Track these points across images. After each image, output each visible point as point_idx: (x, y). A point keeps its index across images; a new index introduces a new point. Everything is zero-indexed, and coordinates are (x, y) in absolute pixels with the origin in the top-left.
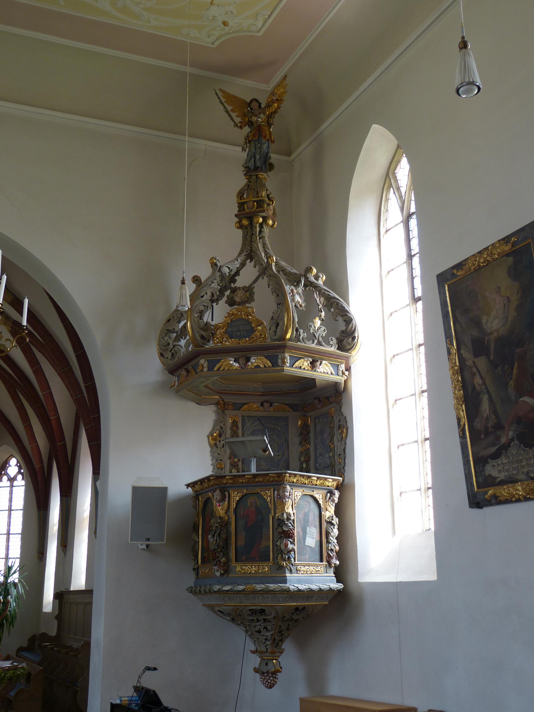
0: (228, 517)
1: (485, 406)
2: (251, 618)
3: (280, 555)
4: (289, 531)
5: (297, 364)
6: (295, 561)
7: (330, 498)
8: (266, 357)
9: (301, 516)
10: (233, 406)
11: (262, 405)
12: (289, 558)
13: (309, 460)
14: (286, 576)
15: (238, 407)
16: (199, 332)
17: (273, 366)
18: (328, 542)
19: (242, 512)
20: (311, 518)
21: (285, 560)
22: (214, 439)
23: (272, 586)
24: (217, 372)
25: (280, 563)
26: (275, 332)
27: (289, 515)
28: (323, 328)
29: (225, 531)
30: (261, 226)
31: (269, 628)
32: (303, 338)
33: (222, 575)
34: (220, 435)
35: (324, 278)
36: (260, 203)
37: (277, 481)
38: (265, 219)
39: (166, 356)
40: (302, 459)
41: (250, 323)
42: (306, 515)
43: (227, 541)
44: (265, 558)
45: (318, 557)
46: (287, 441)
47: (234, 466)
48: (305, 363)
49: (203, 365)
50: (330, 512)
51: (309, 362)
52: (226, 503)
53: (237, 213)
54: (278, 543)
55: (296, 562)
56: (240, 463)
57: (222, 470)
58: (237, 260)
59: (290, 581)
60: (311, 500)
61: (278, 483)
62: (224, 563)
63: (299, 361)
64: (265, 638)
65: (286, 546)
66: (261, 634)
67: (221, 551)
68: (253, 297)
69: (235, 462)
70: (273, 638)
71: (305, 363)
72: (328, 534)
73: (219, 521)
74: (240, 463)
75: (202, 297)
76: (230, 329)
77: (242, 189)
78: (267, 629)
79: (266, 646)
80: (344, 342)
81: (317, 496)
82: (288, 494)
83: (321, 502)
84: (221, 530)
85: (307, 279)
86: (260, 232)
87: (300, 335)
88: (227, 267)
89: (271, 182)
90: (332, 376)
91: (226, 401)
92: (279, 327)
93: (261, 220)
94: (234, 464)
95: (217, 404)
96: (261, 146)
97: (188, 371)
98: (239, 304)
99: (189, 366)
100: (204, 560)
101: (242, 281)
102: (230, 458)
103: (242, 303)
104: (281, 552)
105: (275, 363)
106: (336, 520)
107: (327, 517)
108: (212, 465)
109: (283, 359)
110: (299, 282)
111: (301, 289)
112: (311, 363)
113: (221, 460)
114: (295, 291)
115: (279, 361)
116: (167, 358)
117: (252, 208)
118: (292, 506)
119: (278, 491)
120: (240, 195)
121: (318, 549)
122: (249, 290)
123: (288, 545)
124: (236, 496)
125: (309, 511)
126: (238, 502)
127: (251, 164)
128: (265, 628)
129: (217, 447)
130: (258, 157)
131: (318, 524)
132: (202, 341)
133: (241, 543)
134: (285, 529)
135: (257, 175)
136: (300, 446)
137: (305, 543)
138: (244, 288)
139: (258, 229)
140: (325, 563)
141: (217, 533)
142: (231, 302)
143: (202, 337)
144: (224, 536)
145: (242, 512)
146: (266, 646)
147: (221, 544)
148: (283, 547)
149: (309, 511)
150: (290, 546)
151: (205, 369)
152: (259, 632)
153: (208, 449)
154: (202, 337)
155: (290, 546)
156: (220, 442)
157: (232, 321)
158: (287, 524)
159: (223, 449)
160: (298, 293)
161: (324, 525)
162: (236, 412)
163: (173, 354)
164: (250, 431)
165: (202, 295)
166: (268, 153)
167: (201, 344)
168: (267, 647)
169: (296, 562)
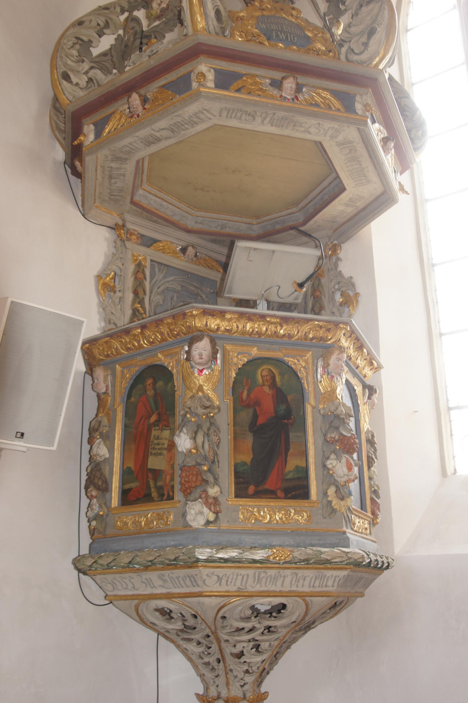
2: (241, 625)
10: (138, 238)
11: (184, 250)
15: (149, 242)
22: (105, 286)
26: (366, 45)
31: (264, 646)
33: (208, 523)
37: (321, 339)
39: (74, 79)
64: (246, 667)
66: (242, 660)
67: (209, 470)
70: (261, 669)
78: (257, 650)
79: (242, 686)
91: (129, 226)
95: (114, 228)
97: (144, 100)
99: (152, 90)
100: (127, 498)
116: (77, 84)
128: (257, 647)
140: (369, 514)
146: (242, 686)
151: (211, 84)
152: (241, 654)
159: (119, 306)
162: (143, 249)
163: (90, 80)
164: (161, 289)
167: (211, 28)
168: (246, 687)
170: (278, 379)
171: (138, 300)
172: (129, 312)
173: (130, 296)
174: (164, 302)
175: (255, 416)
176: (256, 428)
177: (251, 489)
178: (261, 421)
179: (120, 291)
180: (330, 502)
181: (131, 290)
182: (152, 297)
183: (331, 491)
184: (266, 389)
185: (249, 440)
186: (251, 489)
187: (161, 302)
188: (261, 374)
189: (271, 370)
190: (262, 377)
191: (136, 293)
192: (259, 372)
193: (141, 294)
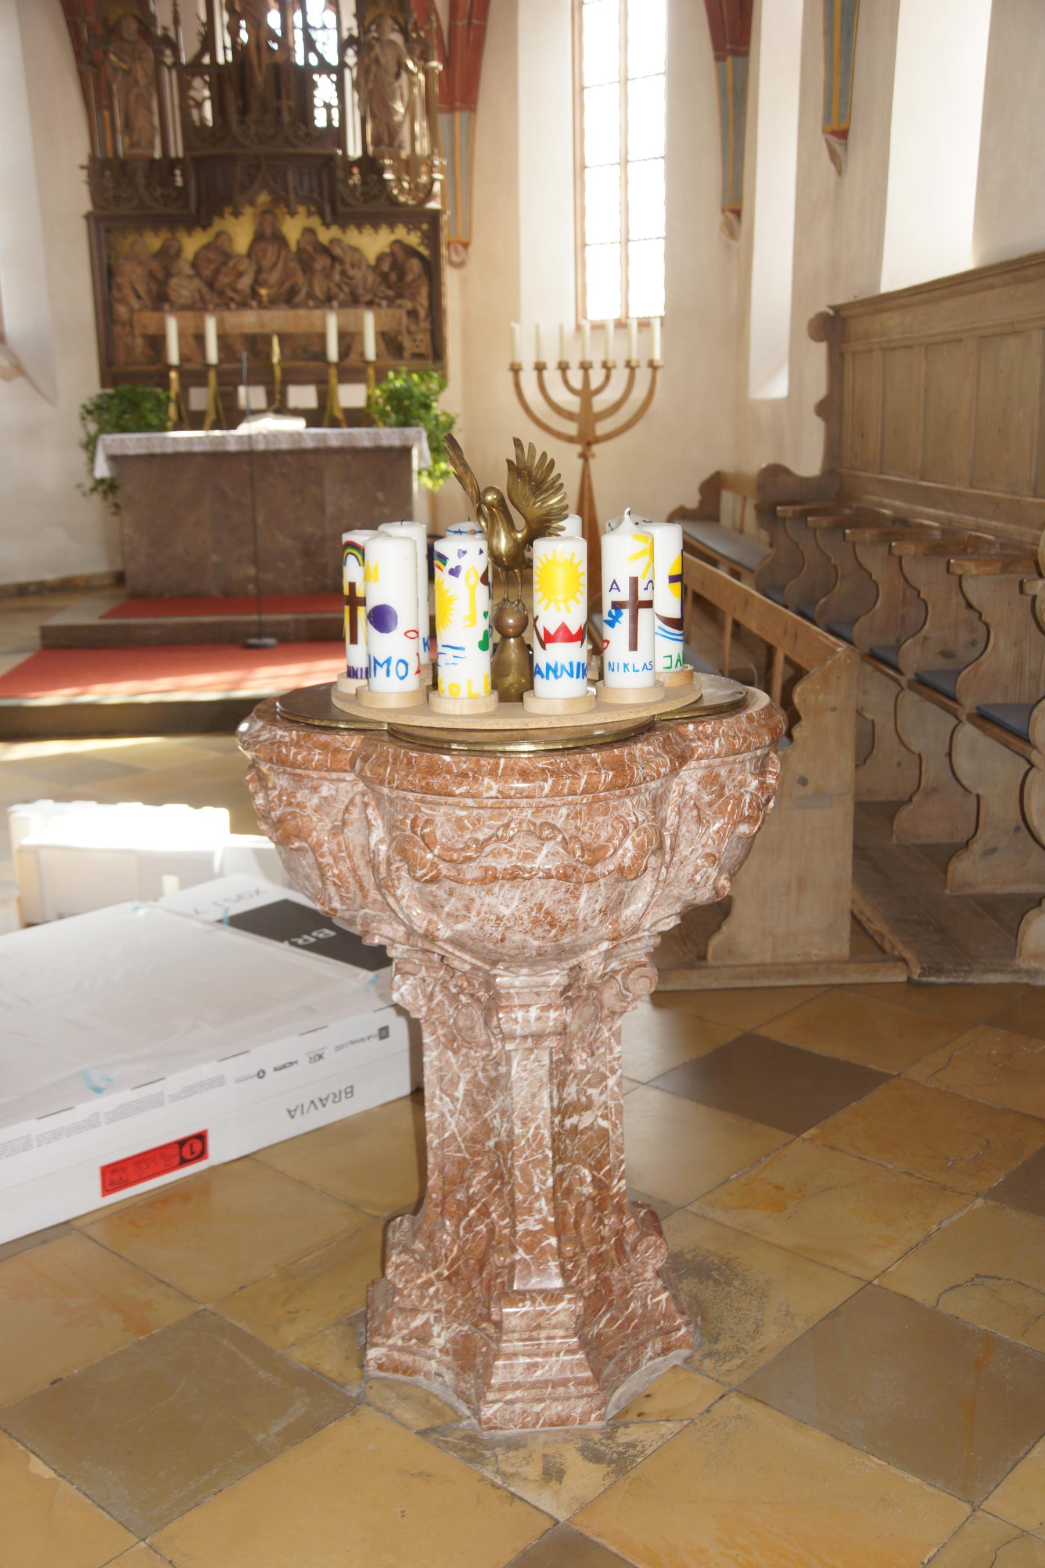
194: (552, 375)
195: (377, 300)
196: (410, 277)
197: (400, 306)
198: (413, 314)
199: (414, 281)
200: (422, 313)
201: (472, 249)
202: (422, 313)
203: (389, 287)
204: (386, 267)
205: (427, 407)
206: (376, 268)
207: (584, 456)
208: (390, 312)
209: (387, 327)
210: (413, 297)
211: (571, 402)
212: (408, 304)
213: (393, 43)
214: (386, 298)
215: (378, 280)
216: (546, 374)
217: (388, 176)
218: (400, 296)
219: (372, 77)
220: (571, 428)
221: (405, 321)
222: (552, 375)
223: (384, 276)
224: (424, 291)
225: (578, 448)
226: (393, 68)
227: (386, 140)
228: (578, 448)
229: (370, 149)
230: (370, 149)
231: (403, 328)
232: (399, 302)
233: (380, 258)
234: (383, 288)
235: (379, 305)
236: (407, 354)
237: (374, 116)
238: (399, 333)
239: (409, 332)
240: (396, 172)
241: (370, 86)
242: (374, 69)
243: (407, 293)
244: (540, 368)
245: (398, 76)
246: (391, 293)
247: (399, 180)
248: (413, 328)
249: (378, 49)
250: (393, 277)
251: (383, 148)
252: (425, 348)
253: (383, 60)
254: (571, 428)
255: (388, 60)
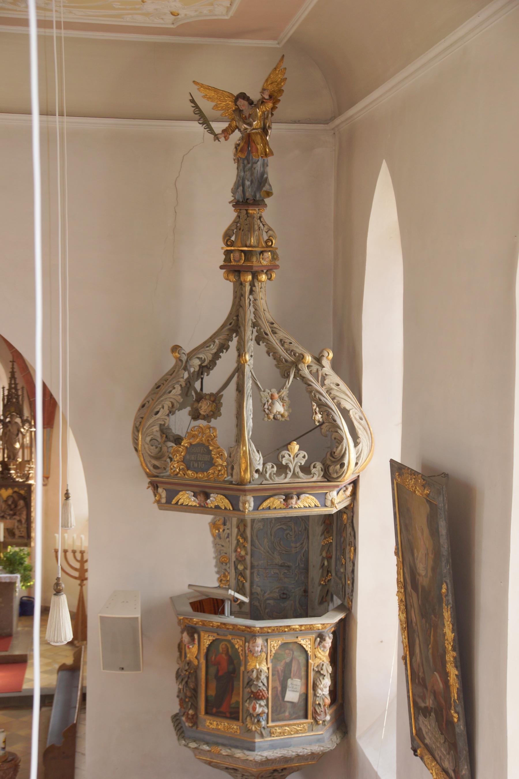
0: (198, 662)
1: (417, 651)
3: (248, 718)
4: (257, 692)
5: (265, 504)
6: (268, 723)
7: (319, 644)
8: (226, 496)
9: (280, 667)
12: (259, 721)
13: (331, 558)
14: (255, 742)
16: (150, 461)
17: (234, 509)
18: (315, 695)
19: (213, 658)
20: (294, 667)
21: (253, 723)
23: (239, 754)
24: (176, 506)
25: (248, 726)
27: (259, 672)
28: (303, 453)
29: (193, 679)
30: (252, 285)
32: (270, 474)
34: (224, 524)
35: (331, 355)
36: (248, 255)
38: (255, 275)
40: (324, 554)
41: (210, 452)
42: (288, 665)
43: (195, 691)
44: (234, 715)
45: (302, 713)
46: (306, 529)
47: (240, 561)
48: (277, 502)
49: (160, 495)
50: (322, 657)
51: (282, 500)
52: (196, 646)
53: (222, 263)
54: (246, 704)
55: (270, 724)
56: (248, 558)
57: (226, 564)
58: (214, 342)
59: (260, 747)
60: (295, 647)
61: (250, 635)
62: (193, 716)
63: (268, 501)
65: (254, 709)
68: (219, 410)
69: (242, 557)
71: (277, 502)
72: (315, 687)
73: (187, 668)
74: (248, 558)
75: (157, 413)
76: (188, 457)
77: (229, 229)
80: (331, 469)
81: (302, 642)
82: (259, 649)
83: (308, 649)
84: (189, 678)
85: (298, 370)
86: (251, 292)
87: (266, 472)
88: (198, 358)
89: (270, 213)
90: (316, 509)
92: (235, 471)
93: (250, 278)
94: (240, 559)
96: (252, 167)
98: (205, 418)
101: (211, 383)
102: (236, 551)
103: (207, 418)
104: (251, 715)
105: (235, 507)
106: (328, 669)
107: (316, 665)
108: (214, 558)
109: (244, 503)
110: (288, 377)
111: (285, 392)
112: (284, 500)
113: (226, 553)
114: (276, 396)
115: (241, 505)
117: (239, 261)
118: (267, 659)
119: (249, 642)
120: (227, 236)
121: (303, 703)
122: (216, 399)
123: (256, 708)
124: (207, 640)
125: (291, 661)
126: (208, 649)
127: (239, 196)
129: (220, 538)
130: (248, 183)
131: (303, 673)
132: (155, 470)
133: (212, 693)
134: (254, 690)
135: (247, 210)
136: (323, 537)
137: (283, 697)
138: (211, 395)
139: (248, 288)
140: (310, 720)
141: (186, 679)
142: (196, 416)
143: (155, 467)
144: (192, 685)
145: (213, 658)
147: (188, 694)
148: (251, 711)
149: (291, 661)
150: (259, 710)
153: (210, 539)
154: (155, 467)
155: (259, 710)
156: (224, 530)
157: (191, 444)
158: (257, 685)
159: (228, 540)
160: (282, 399)
161: (312, 675)
165: (156, 410)
166: (263, 173)
169: (270, 724)
170: (230, 650)
171: (240, 533)
172: (235, 542)
173: (235, 531)
174: (264, 526)
175: (218, 671)
176: (218, 678)
177: (214, 710)
178: (220, 673)
179: (228, 529)
180: (247, 725)
181: (235, 527)
182: (254, 525)
183: (248, 718)
184: (224, 655)
185: (213, 685)
186: (214, 710)
187: (262, 527)
188: (222, 647)
189: (226, 645)
190: (222, 648)
191: (238, 527)
192: (221, 646)
193: (242, 529)
194: (70, 555)
195: (6, 516)
196: (19, 507)
197: (15, 519)
198: (20, 521)
199: (21, 509)
200: (24, 521)
201: (50, 479)
202: (24, 521)
203: (11, 510)
204: (10, 502)
205: (22, 564)
206: (6, 501)
207: (81, 585)
208: (10, 521)
209: (10, 526)
210: (20, 514)
211: (77, 565)
212: (18, 518)
213: (16, 423)
214: (9, 515)
215: (7, 507)
216: (68, 553)
217: (12, 472)
218: (15, 514)
219: (7, 436)
220: (76, 574)
221: (16, 524)
222: (70, 555)
223: (9, 506)
224: (25, 513)
225: (78, 582)
226: (16, 432)
227: (12, 457)
228: (78, 582)
229: (6, 460)
230: (6, 460)
231: (16, 527)
232: (15, 517)
233: (9, 497)
234: (8, 511)
235: (6, 518)
236: (17, 537)
237: (8, 449)
238: (13, 529)
239: (18, 528)
240: (15, 470)
241: (6, 439)
242: (8, 433)
243: (18, 513)
244: (65, 551)
245: (18, 435)
246: (11, 512)
247: (17, 473)
248: (20, 527)
249: (10, 427)
250: (13, 506)
251: (10, 460)
252: (24, 534)
253: (12, 430)
254: (76, 574)
255: (14, 430)
